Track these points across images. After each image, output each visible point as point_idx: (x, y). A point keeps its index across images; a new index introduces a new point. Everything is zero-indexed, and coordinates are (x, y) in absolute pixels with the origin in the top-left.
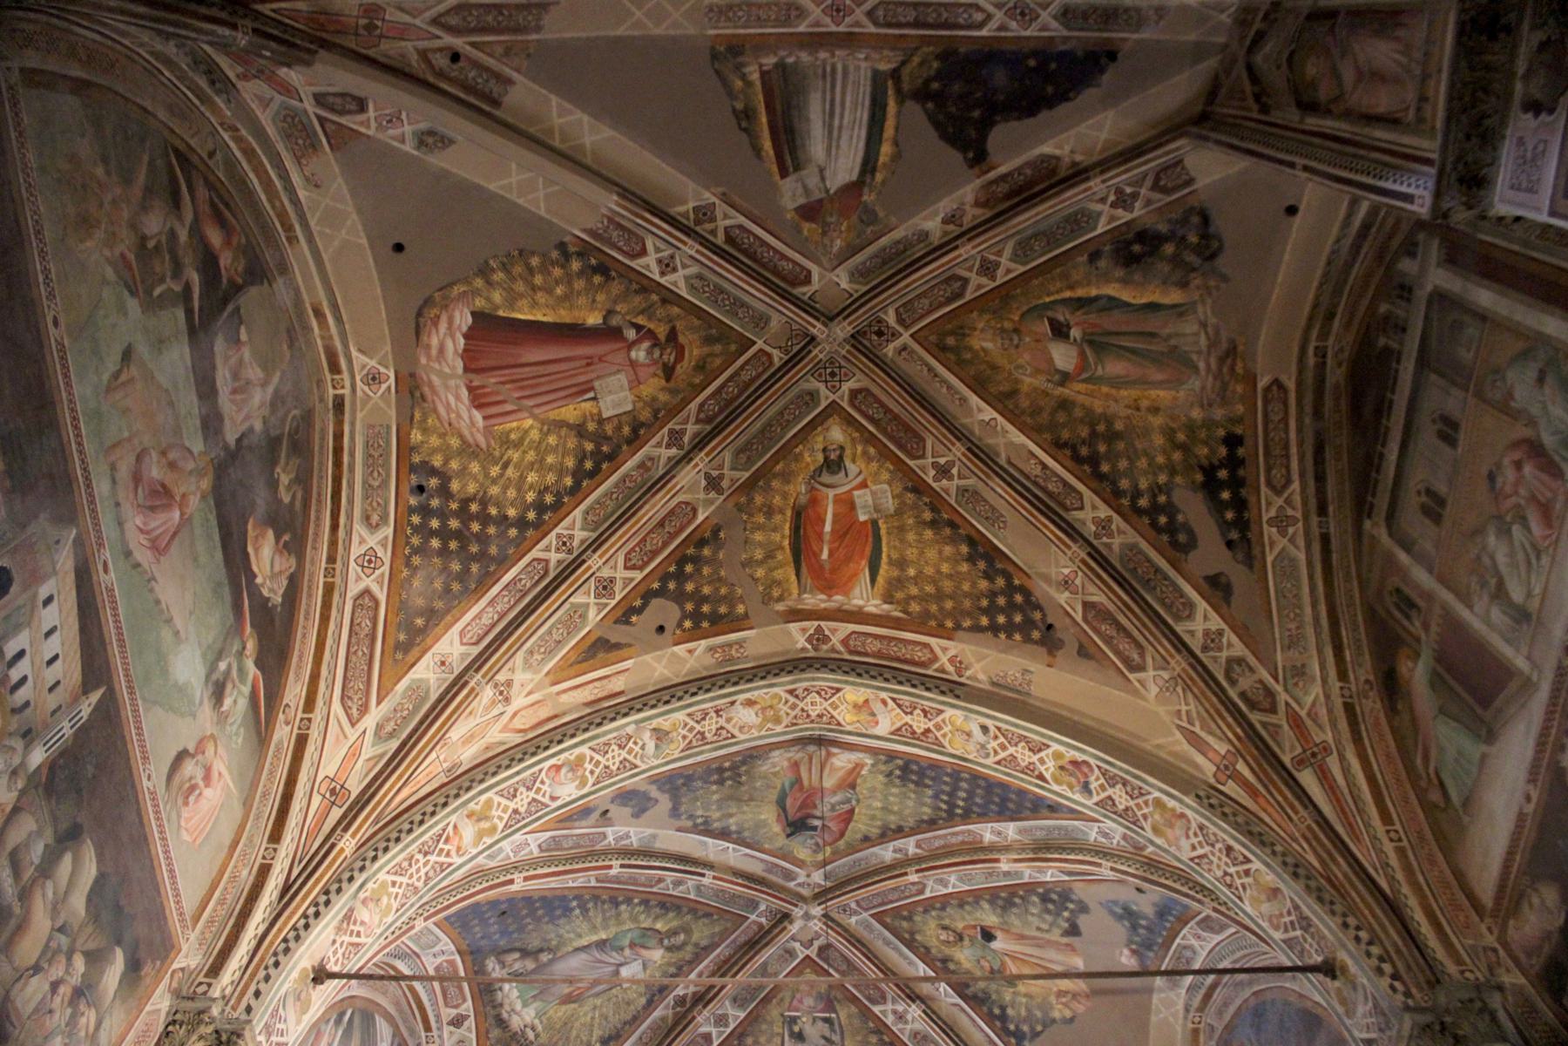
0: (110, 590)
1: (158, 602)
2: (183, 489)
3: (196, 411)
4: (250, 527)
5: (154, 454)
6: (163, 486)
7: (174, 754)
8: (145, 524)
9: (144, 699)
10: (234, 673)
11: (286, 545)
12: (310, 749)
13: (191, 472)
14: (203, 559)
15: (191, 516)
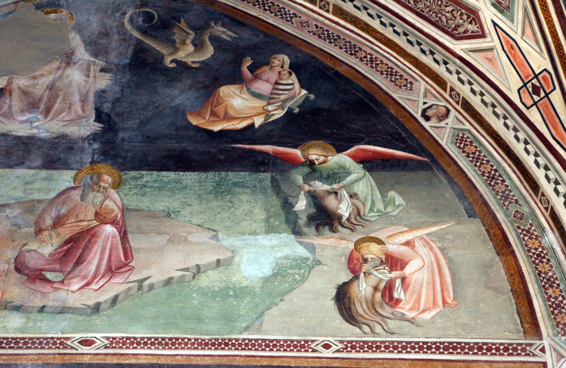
0: (113, 342)
1: (168, 282)
2: (91, 216)
3: (31, 172)
4: (194, 121)
5: (33, 246)
6: (66, 242)
7: (331, 304)
8: (84, 277)
9: (246, 329)
10: (320, 186)
11: (252, 69)
12: (475, 101)
13: (83, 198)
14: (176, 205)
15: (124, 210)
